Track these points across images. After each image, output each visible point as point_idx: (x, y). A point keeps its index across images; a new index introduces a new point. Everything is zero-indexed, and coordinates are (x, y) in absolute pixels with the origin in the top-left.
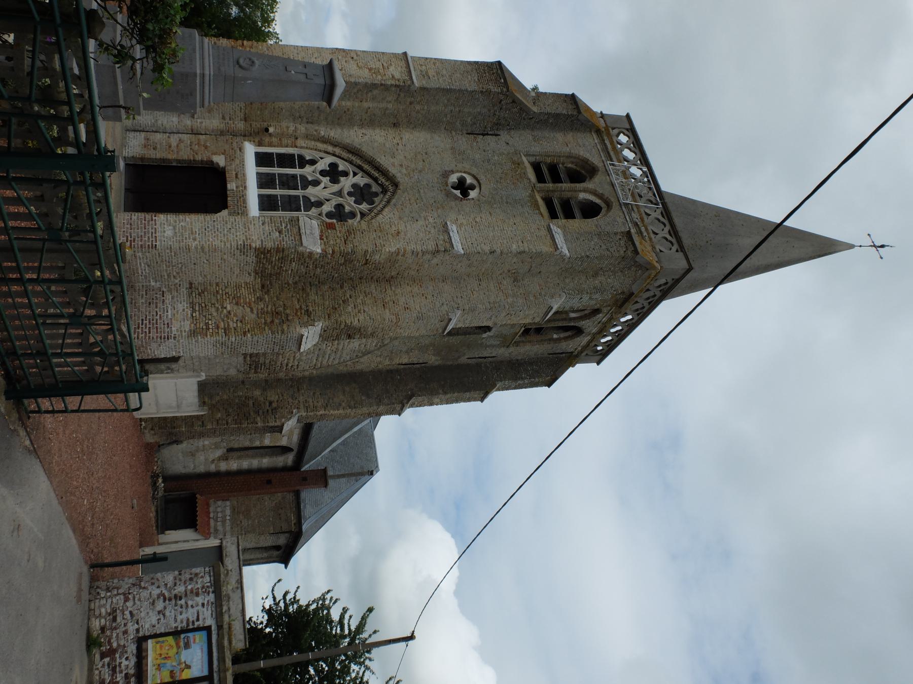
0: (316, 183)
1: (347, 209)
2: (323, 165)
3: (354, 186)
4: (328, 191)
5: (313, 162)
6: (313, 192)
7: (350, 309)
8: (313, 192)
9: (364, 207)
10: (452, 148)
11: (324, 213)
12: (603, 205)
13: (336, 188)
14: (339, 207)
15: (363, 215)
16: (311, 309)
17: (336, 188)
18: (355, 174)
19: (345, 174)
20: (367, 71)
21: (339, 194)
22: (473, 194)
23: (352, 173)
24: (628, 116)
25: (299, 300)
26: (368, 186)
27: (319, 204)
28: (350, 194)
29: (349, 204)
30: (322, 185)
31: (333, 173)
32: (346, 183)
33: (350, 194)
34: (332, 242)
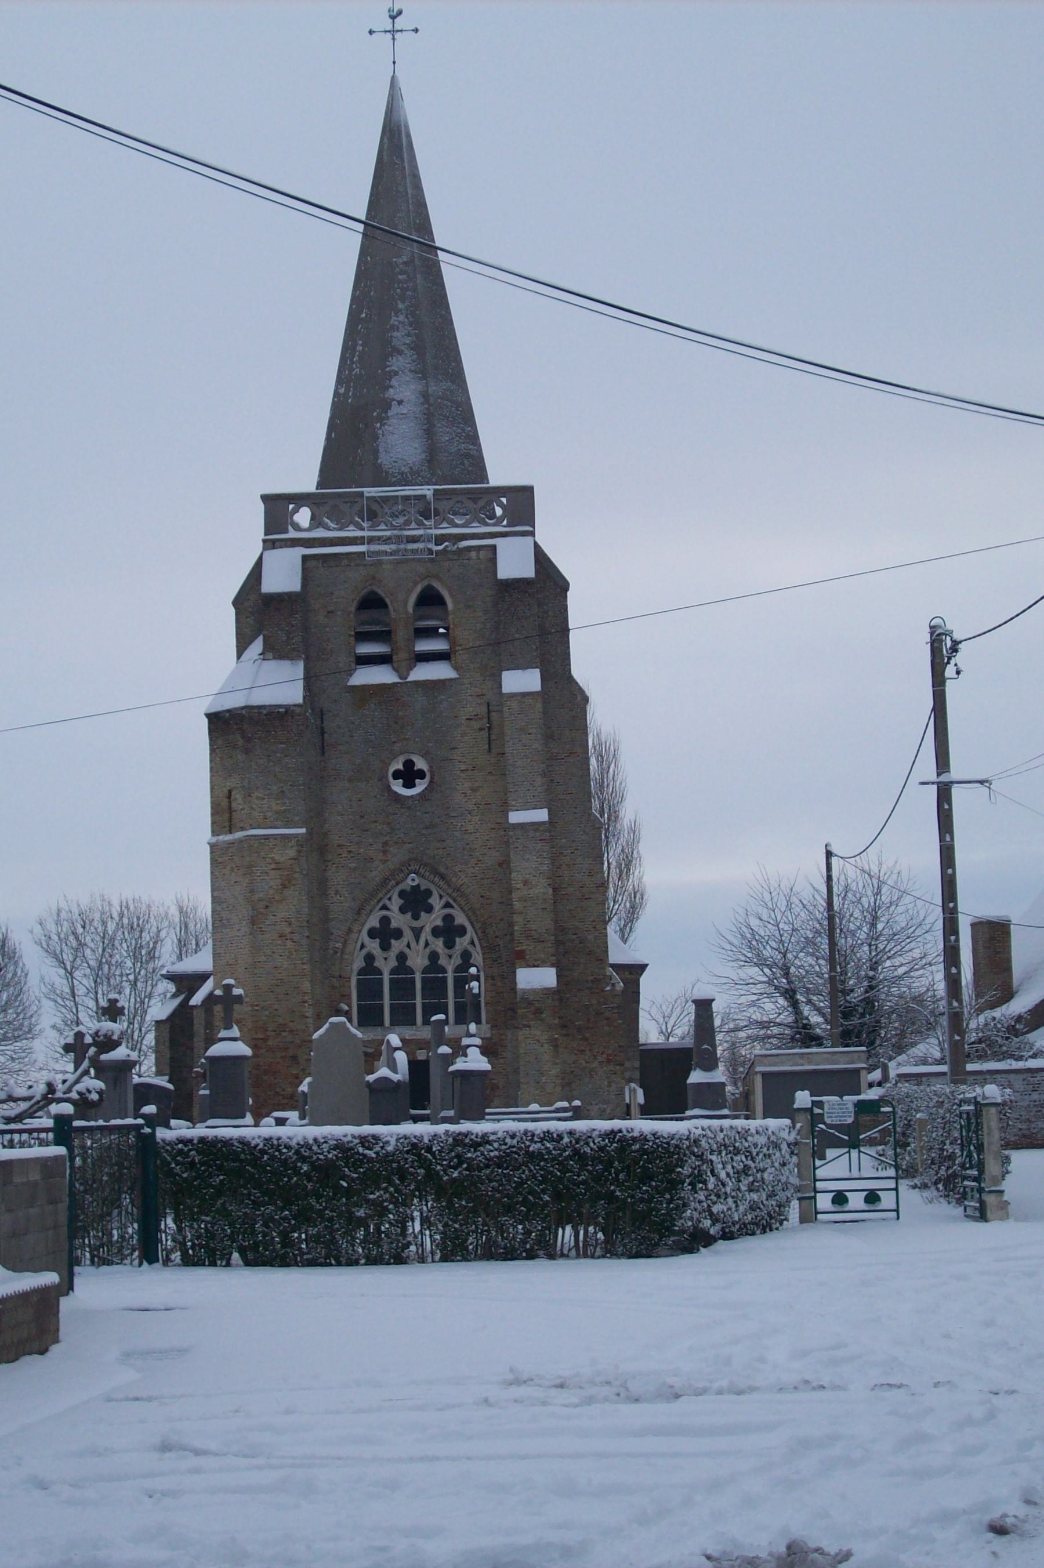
0: (402, 957)
1: (439, 922)
2: (373, 946)
3: (403, 910)
4: (413, 944)
5: (370, 958)
6: (418, 961)
7: (590, 937)
8: (418, 961)
9: (435, 901)
10: (350, 780)
11: (447, 951)
12: (425, 583)
13: (408, 935)
14: (436, 932)
15: (447, 905)
16: (591, 978)
17: (408, 935)
18: (385, 907)
19: (385, 921)
20: (287, 892)
21: (417, 933)
22: (421, 764)
23: (384, 912)
24: (265, 498)
25: (579, 990)
26: (402, 894)
27: (434, 956)
28: (416, 917)
29: (433, 919)
30: (407, 951)
31: (385, 934)
32: (399, 920)
33: (416, 917)
34: (542, 956)
